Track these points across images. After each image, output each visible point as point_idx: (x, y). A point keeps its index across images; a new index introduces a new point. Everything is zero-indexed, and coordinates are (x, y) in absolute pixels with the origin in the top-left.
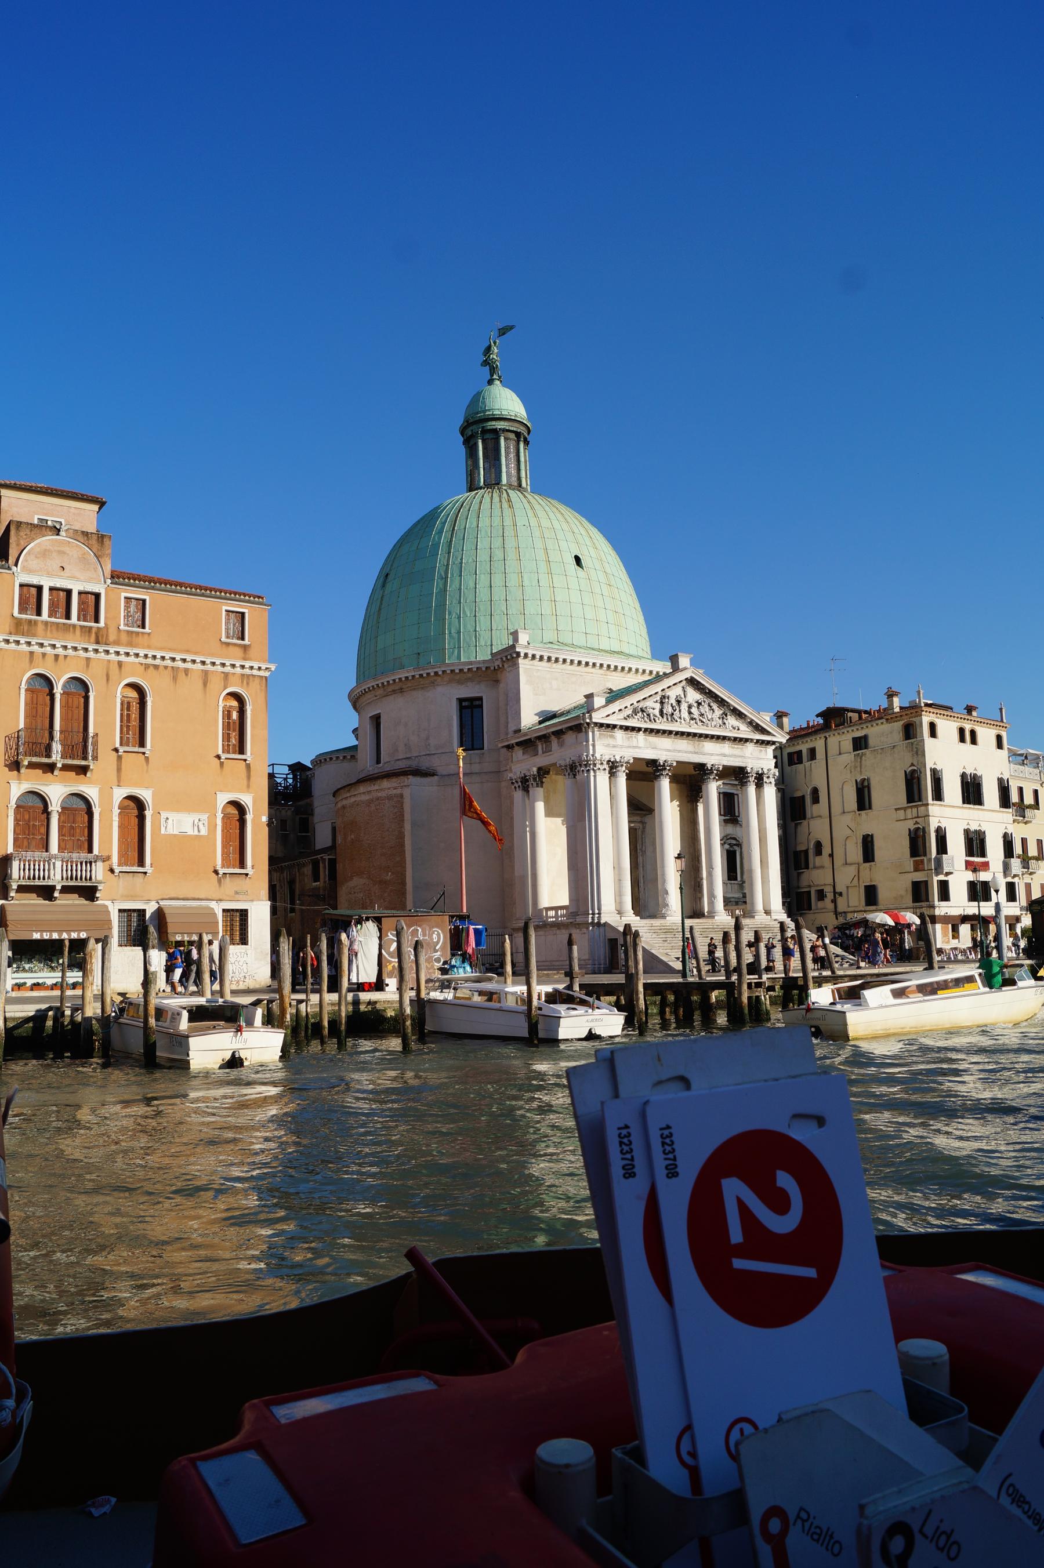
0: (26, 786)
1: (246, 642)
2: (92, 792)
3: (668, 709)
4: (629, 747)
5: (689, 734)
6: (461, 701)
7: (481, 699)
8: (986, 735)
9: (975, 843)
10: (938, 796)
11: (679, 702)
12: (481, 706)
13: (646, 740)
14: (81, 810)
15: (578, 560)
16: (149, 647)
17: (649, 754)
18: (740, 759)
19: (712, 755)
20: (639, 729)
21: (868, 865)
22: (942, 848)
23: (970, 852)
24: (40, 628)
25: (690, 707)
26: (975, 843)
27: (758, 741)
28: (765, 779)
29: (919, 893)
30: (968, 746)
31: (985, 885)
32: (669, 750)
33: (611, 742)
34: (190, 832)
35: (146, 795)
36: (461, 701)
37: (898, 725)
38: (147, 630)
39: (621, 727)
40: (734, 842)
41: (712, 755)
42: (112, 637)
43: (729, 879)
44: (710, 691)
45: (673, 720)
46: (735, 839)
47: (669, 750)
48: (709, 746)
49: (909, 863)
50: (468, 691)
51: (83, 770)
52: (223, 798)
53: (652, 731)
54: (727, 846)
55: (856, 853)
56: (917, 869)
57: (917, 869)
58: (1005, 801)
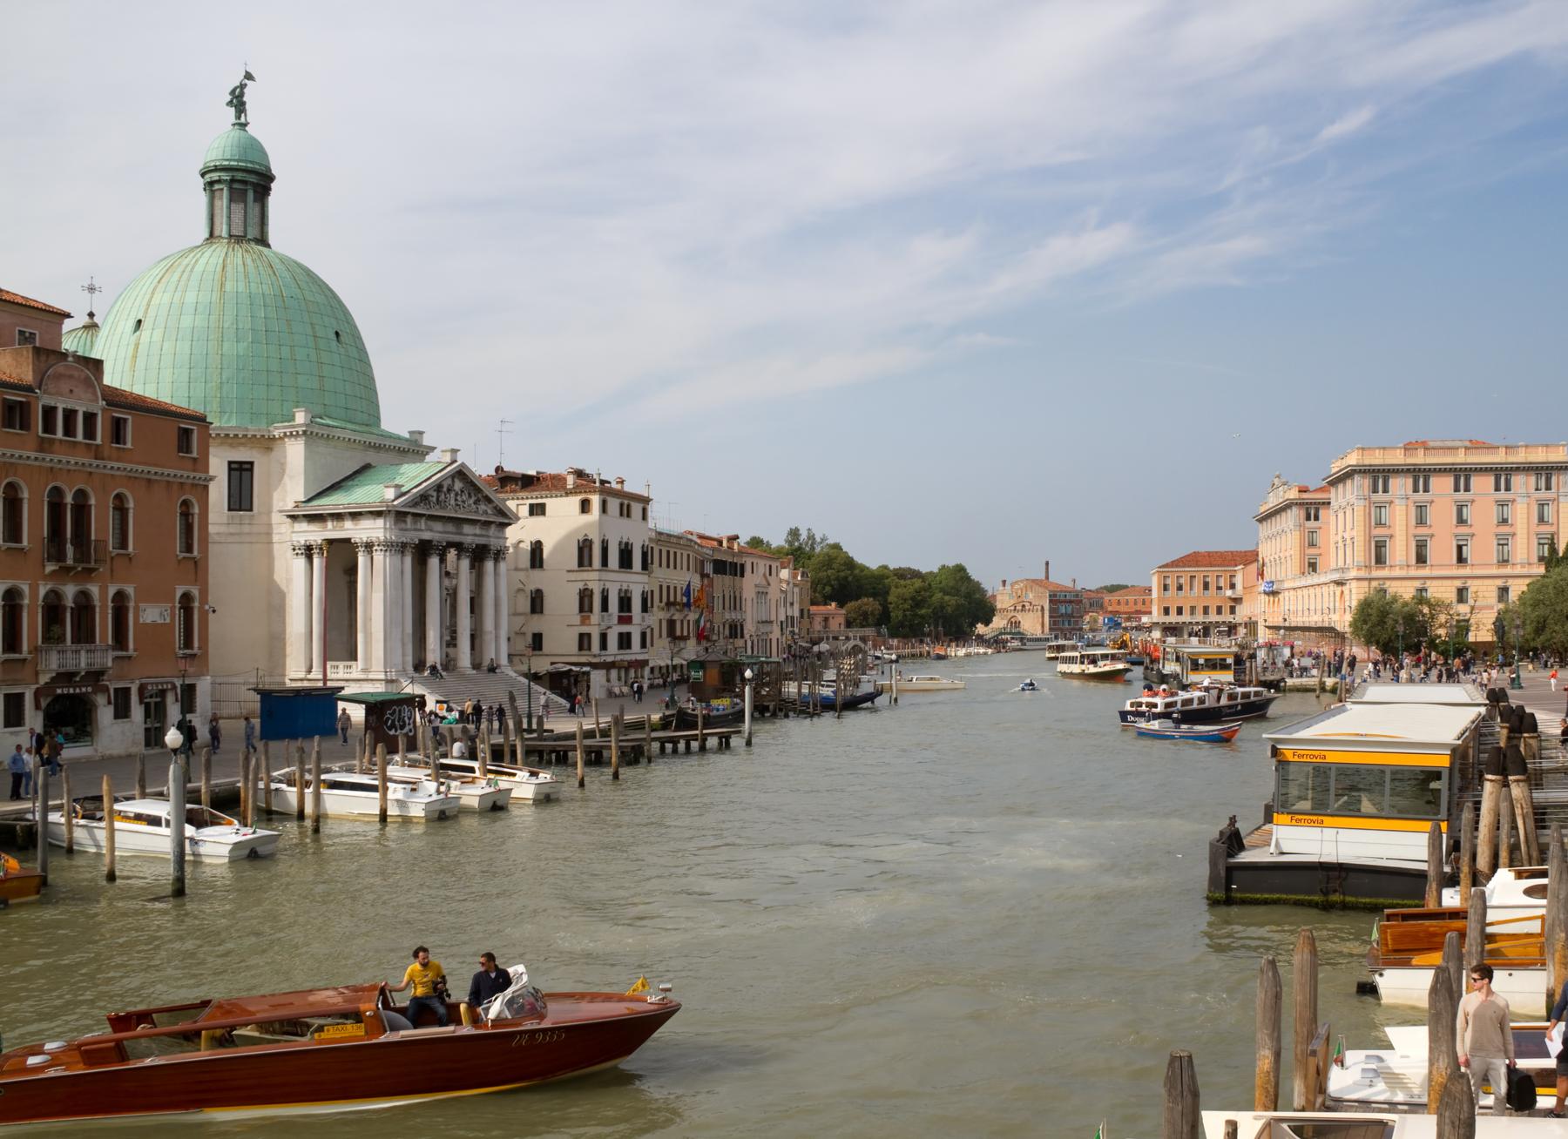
0: (48, 587)
1: (195, 455)
2: (94, 590)
3: (442, 497)
6: (230, 463)
7: (252, 463)
8: (636, 508)
9: (625, 603)
10: (605, 562)
11: (449, 490)
12: (251, 470)
14: (84, 607)
16: (131, 462)
17: (427, 536)
21: (536, 616)
22: (605, 608)
23: (621, 609)
24: (57, 445)
26: (625, 603)
29: (584, 641)
30: (625, 520)
31: (629, 635)
35: (130, 590)
36: (230, 463)
37: (575, 501)
38: (129, 445)
42: (106, 453)
45: (445, 508)
48: (467, 529)
49: (577, 619)
50: (241, 455)
51: (91, 570)
55: (525, 604)
56: (583, 623)
57: (583, 623)
58: (645, 566)
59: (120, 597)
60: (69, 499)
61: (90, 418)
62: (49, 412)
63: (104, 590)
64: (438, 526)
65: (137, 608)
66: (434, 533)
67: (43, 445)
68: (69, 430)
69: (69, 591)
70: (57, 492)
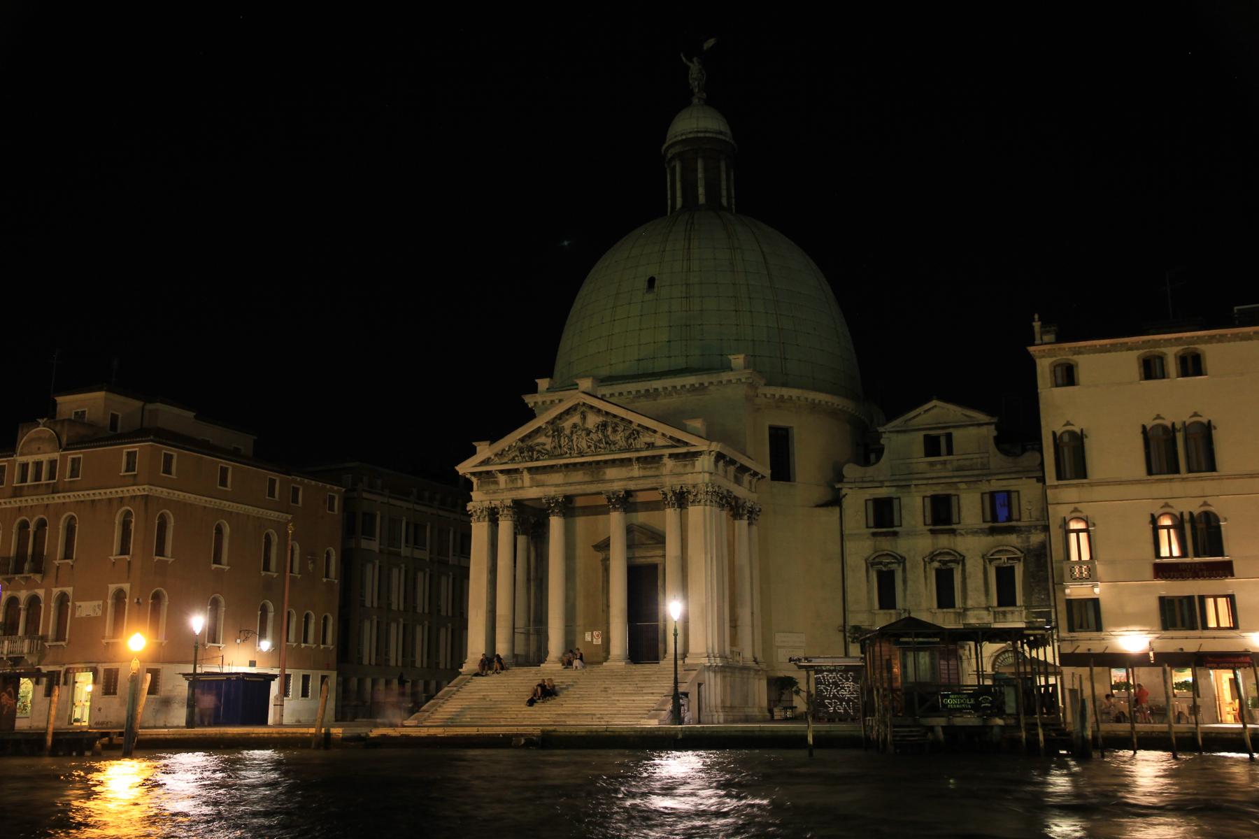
2: (41, 593)
4: (511, 489)
5: (583, 464)
11: (572, 433)
13: (532, 479)
15: (651, 282)
18: (654, 480)
19: (612, 481)
20: (516, 471)
25: (588, 434)
27: (671, 456)
28: (691, 498)
32: (557, 485)
33: (493, 487)
34: (92, 615)
35: (69, 590)
39: (502, 472)
40: (947, 558)
41: (612, 481)
43: (940, 606)
44: (607, 413)
46: (948, 554)
47: (557, 485)
48: (611, 473)
52: (112, 588)
53: (537, 468)
54: (936, 564)
59: (63, 599)
60: (32, 529)
61: (53, 463)
62: (25, 466)
63: (48, 593)
64: (557, 478)
65: (74, 604)
66: (551, 487)
67: (17, 493)
68: (38, 477)
69: (23, 595)
70: (24, 526)
